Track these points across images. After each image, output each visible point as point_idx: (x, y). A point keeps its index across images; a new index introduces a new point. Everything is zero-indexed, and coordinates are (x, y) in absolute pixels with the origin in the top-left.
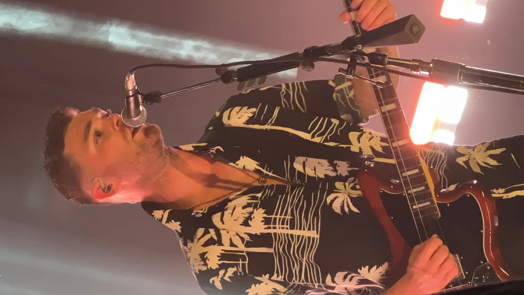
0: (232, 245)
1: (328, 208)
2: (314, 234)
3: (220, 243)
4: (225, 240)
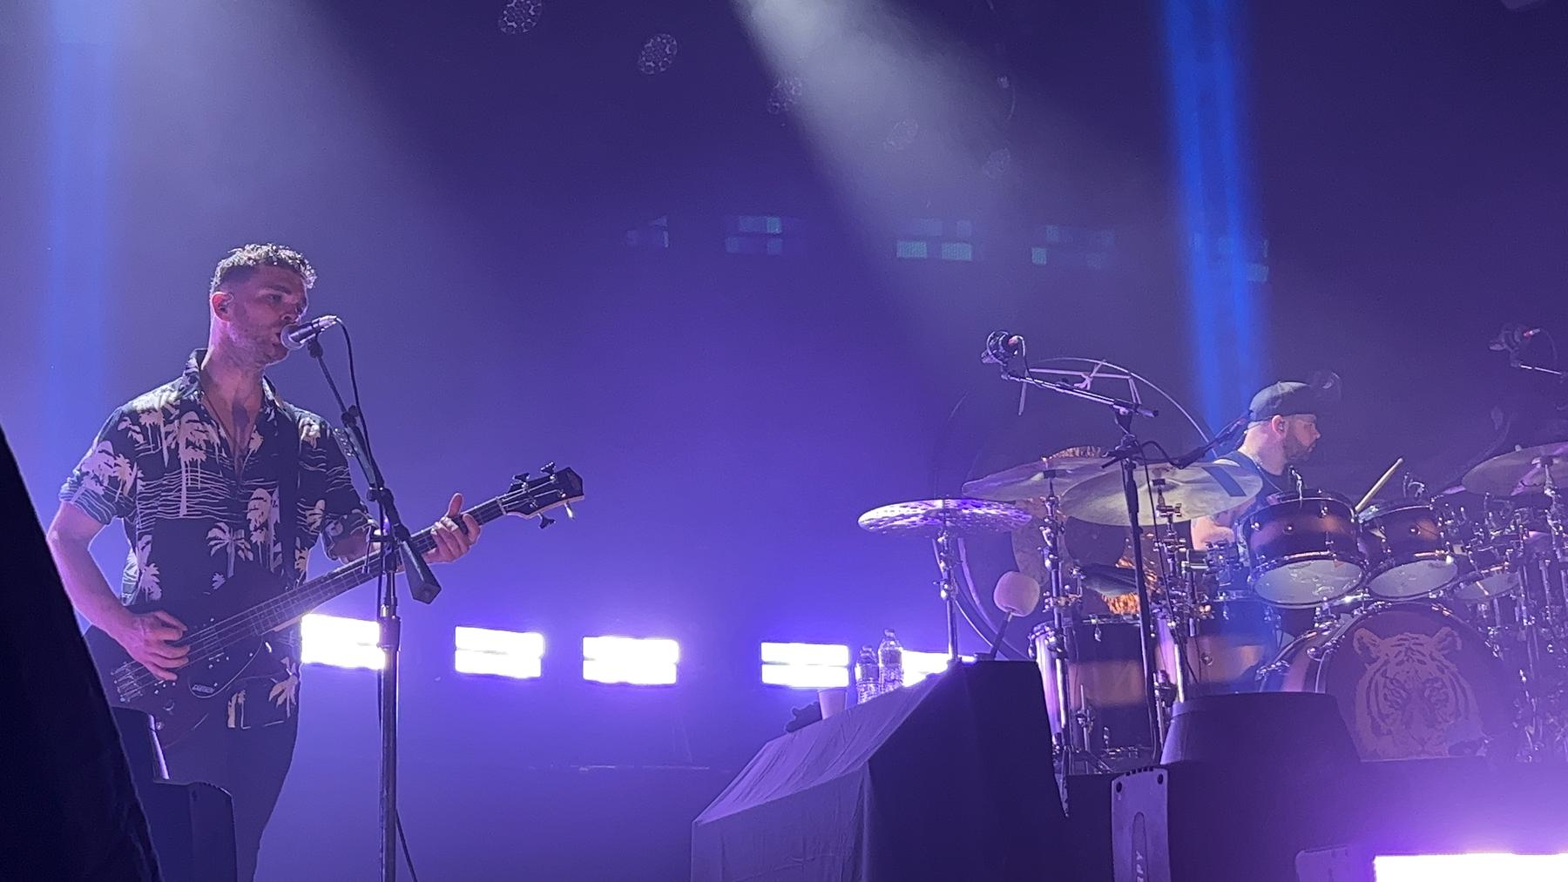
0: (167, 434)
1: (213, 525)
2: (183, 511)
3: (168, 422)
4: (169, 428)
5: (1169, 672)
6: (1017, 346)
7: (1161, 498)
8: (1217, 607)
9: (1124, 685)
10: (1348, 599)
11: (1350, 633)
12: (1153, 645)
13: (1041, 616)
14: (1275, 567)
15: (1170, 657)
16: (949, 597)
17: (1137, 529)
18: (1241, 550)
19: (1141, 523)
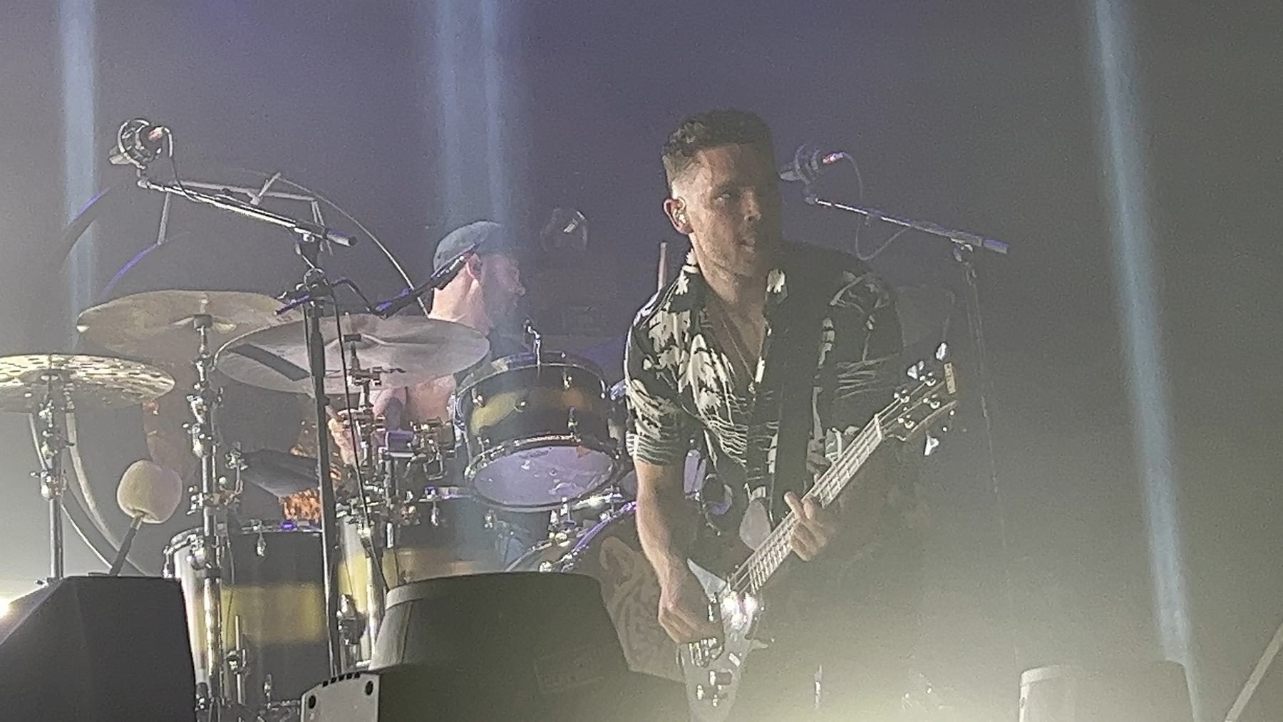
5: (357, 597)
6: (160, 142)
7: (355, 360)
8: (425, 509)
9: (304, 613)
10: (594, 501)
11: (595, 542)
12: (337, 556)
13: (184, 521)
14: (504, 454)
15: (357, 573)
16: (52, 496)
17: (323, 400)
18: (458, 432)
19: (327, 391)
